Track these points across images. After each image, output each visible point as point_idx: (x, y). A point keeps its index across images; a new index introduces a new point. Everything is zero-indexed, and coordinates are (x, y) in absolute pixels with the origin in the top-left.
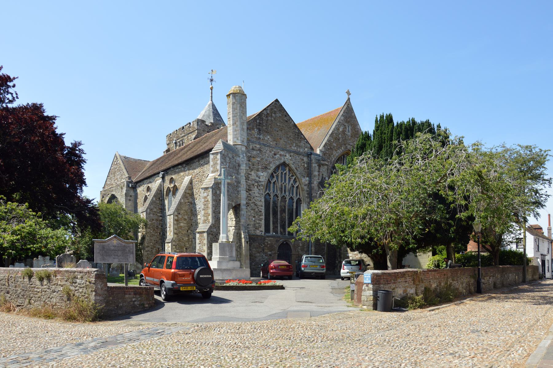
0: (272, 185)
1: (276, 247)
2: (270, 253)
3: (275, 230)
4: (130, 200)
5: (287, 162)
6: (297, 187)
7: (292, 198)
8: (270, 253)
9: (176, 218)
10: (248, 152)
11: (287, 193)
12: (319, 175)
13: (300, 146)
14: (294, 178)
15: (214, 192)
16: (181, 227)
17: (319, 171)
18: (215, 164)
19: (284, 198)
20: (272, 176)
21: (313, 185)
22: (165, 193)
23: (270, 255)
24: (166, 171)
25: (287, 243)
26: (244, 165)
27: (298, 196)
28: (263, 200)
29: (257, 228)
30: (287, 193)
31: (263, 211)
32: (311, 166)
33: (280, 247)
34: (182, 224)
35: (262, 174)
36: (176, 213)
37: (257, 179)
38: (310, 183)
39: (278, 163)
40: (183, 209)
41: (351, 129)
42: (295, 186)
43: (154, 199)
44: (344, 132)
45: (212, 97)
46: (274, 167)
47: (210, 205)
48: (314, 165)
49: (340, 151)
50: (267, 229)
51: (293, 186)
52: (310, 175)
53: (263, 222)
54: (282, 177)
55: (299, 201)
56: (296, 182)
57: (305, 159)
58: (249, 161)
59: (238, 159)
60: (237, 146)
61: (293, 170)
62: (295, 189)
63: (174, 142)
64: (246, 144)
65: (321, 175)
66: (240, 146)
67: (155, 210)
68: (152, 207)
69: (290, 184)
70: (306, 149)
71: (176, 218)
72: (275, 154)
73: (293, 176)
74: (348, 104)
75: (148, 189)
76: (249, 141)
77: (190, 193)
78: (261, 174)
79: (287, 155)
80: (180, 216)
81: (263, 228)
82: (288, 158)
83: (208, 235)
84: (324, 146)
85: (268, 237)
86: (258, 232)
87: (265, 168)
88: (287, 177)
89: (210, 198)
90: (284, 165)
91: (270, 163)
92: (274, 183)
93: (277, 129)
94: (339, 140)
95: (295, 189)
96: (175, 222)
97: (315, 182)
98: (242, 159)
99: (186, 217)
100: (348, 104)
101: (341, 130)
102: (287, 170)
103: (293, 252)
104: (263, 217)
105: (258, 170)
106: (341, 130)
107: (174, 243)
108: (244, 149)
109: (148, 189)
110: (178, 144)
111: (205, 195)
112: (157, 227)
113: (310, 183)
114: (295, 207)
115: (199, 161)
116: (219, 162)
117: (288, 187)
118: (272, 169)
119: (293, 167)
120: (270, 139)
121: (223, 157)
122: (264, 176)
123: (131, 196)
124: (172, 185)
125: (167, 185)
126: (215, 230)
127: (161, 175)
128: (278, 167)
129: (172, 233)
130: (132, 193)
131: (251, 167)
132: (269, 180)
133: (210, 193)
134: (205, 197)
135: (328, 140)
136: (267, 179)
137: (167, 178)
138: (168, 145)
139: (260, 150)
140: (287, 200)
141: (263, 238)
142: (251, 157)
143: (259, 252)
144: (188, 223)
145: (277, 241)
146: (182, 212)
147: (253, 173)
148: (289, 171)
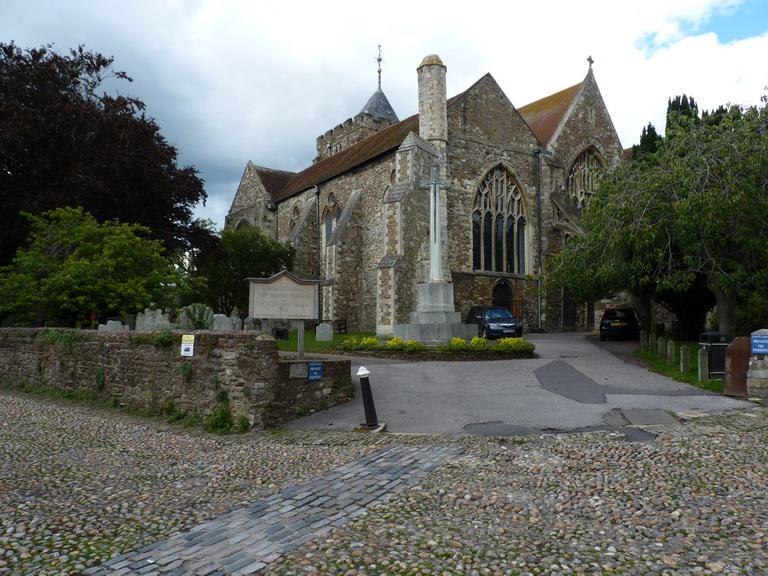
0: (483, 198)
1: (490, 290)
2: (481, 299)
3: (488, 266)
4: (268, 227)
5: (505, 164)
6: (519, 201)
7: (511, 218)
8: (481, 299)
9: (340, 249)
10: (448, 150)
11: (505, 210)
12: (551, 182)
13: (521, 141)
14: (514, 187)
15: (404, 208)
16: (347, 262)
17: (552, 177)
18: (404, 168)
19: (500, 216)
20: (483, 184)
21: (542, 197)
22: (321, 214)
23: (482, 302)
24: (322, 184)
25: (505, 285)
26: (445, 170)
27: (521, 215)
28: (471, 221)
29: (462, 263)
30: (505, 210)
31: (471, 237)
32: (539, 170)
33: (496, 289)
34: (347, 259)
35: (469, 182)
36: (340, 243)
37: (463, 189)
38: (538, 194)
39: (491, 166)
40: (351, 236)
41: (596, 115)
42: (517, 199)
43: (306, 224)
44: (584, 120)
45: (380, 83)
46: (485, 171)
47: (398, 229)
48: (543, 168)
49: (581, 148)
50: (477, 265)
51: (513, 200)
52: (537, 183)
53: (471, 253)
54: (497, 188)
55: (522, 222)
56: (517, 194)
57: (530, 159)
58: (450, 163)
59: (436, 160)
60: (434, 142)
61: (514, 176)
62: (516, 203)
63: (328, 146)
64: (446, 139)
65: (554, 183)
66: (438, 142)
67: (306, 239)
68: (302, 235)
69: (509, 198)
70: (531, 145)
71: (340, 249)
72: (487, 153)
73: (512, 184)
74: (590, 76)
75: (296, 210)
76: (449, 134)
77: (358, 214)
78: (467, 182)
79: (505, 154)
80: (345, 247)
81: (471, 262)
82: (505, 159)
83: (396, 272)
84: (558, 140)
85: (479, 275)
86: (464, 269)
87: (474, 173)
88: (505, 186)
89: (398, 218)
90: (500, 167)
91: (481, 165)
92: (486, 195)
93: (490, 117)
94: (578, 130)
95: (516, 203)
96: (339, 256)
97: (546, 194)
98: (442, 157)
99: (354, 248)
100: (590, 76)
101: (580, 116)
102: (505, 176)
103: (516, 298)
104: (471, 246)
105: (464, 177)
106: (580, 116)
107: (336, 286)
108: (444, 145)
109: (296, 210)
110: (334, 149)
111: (391, 212)
112: (310, 265)
113: (538, 194)
114: (516, 230)
115: (373, 167)
116: (409, 165)
117: (507, 200)
118: (483, 175)
119: (513, 171)
120: (480, 132)
121: (417, 157)
122: (471, 186)
123: (270, 221)
124: (332, 204)
125: (324, 202)
126: (405, 265)
127: (315, 190)
128: (492, 172)
129: (333, 272)
130: (271, 216)
131: (452, 175)
132: (479, 190)
133: (398, 211)
134: (391, 217)
135: (564, 132)
136: (476, 189)
137: (324, 192)
138: (318, 150)
139: (466, 147)
140: (505, 219)
141: (471, 277)
142: (451, 156)
143: (464, 298)
144: (356, 257)
145: (492, 281)
146: (348, 240)
147: (456, 181)
148: (508, 177)
